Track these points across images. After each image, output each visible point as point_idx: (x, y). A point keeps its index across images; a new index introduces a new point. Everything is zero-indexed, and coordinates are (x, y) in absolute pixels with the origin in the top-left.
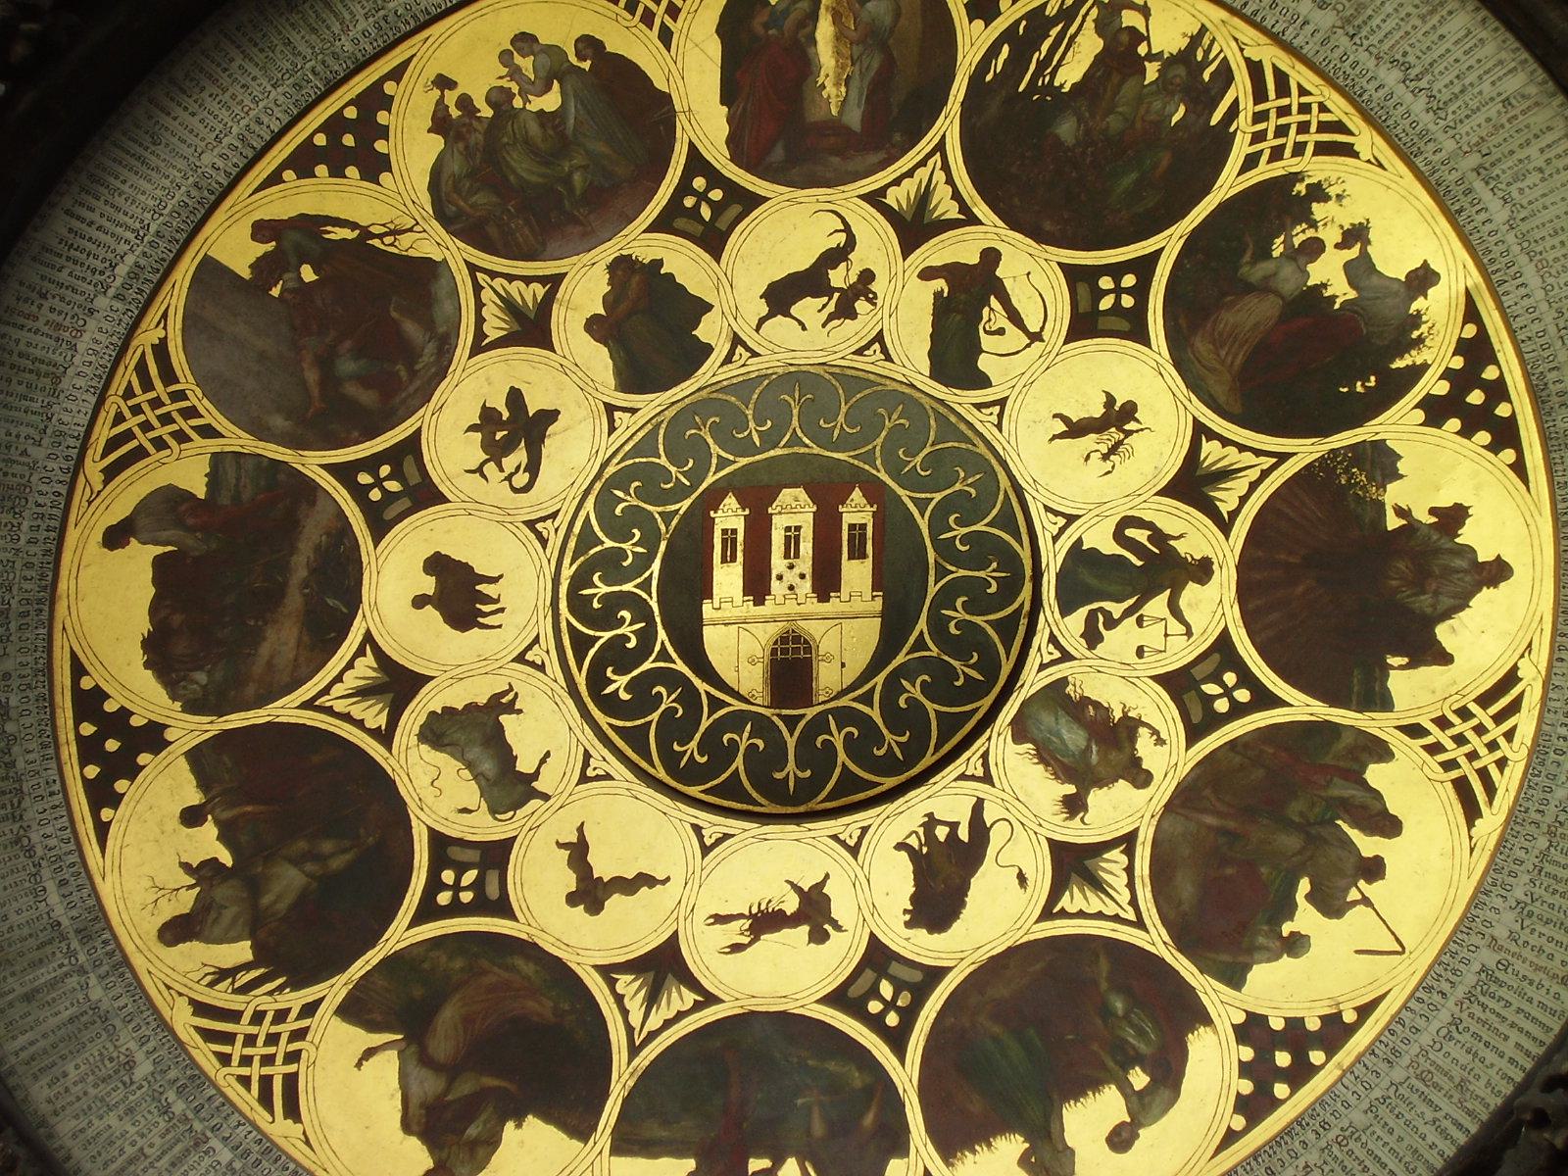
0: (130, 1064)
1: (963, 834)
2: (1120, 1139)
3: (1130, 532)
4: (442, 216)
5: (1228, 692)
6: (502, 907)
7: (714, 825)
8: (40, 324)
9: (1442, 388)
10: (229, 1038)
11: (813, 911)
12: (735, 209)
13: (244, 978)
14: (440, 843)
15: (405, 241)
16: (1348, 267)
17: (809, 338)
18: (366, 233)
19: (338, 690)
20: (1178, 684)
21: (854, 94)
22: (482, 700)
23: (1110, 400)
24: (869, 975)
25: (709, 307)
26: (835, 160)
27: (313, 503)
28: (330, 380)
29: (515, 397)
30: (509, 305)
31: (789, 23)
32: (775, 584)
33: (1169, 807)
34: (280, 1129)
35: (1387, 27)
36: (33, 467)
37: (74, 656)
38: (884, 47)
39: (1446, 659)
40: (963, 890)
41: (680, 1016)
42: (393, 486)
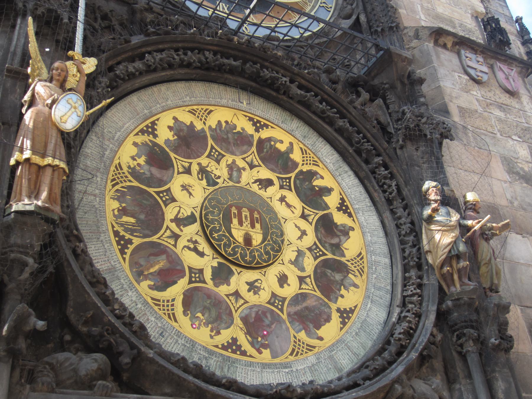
0: (375, 278)
1: (258, 183)
2: (282, 142)
4: (232, 322)
6: (315, 244)
7: (282, 221)
8: (305, 378)
9: (151, 136)
12: (193, 270)
14: (315, 258)
15: (241, 326)
16: (139, 158)
18: (245, 334)
19: (310, 288)
20: (218, 162)
21: (159, 259)
23: (182, 190)
26: (173, 257)
27: (290, 312)
29: (249, 291)
30: (236, 301)
33: (236, 155)
34: (364, 253)
35: (94, 162)
36: (325, 359)
37: (341, 331)
38: (148, 257)
39: (191, 122)
40: (264, 179)
41: (308, 210)
42: (277, 301)
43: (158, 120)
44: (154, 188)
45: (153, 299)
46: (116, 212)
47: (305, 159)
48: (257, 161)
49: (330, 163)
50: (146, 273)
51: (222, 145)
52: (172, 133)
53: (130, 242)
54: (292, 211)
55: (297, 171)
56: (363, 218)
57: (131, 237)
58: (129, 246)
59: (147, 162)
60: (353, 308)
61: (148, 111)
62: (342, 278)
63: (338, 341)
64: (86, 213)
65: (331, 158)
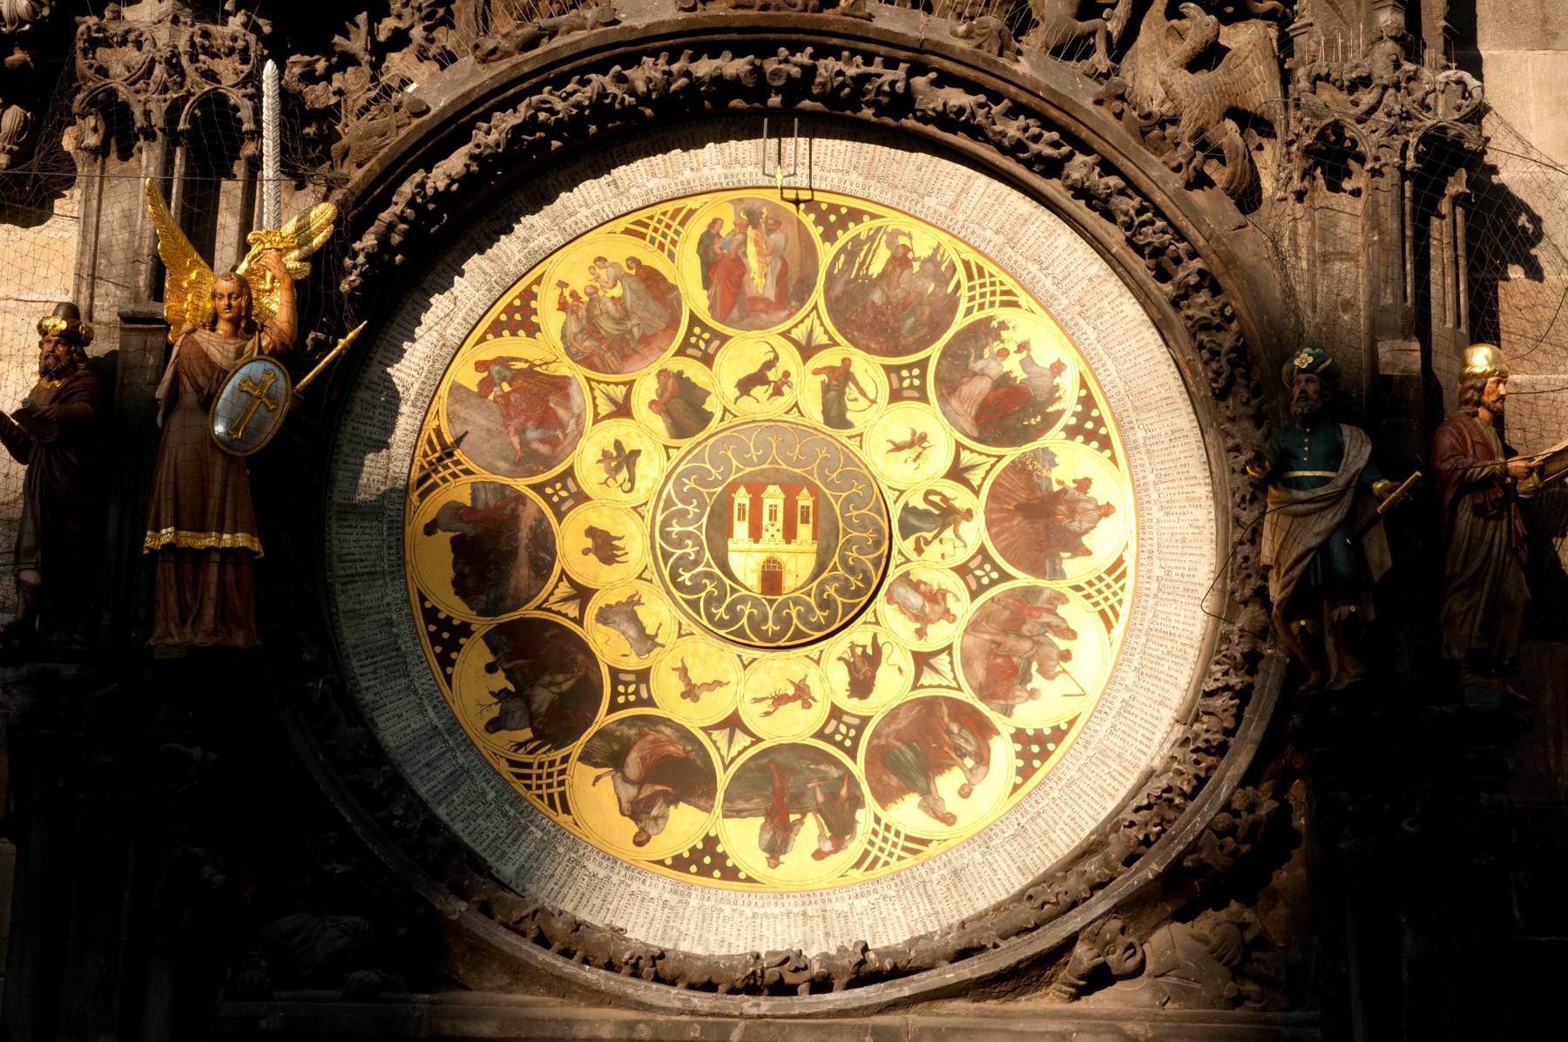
0: (484, 794)
1: (869, 651)
2: (965, 793)
3: (931, 497)
5: (987, 574)
6: (650, 702)
9: (1073, 421)
10: (529, 777)
11: (802, 693)
12: (716, 343)
13: (531, 746)
14: (614, 672)
16: (1022, 362)
17: (760, 404)
18: (533, 365)
19: (552, 599)
20: (962, 570)
22: (624, 600)
23: (914, 433)
24: (833, 723)
25: (708, 393)
26: (764, 316)
28: (525, 444)
31: (733, 246)
32: (764, 533)
33: (966, 631)
38: (783, 259)
39: (1088, 553)
40: (873, 677)
41: (745, 749)
42: (564, 494)
44: (939, 363)
45: (691, 212)
46: (902, 240)
47: (891, 836)
48: (931, 686)
51: (1005, 608)
53: (829, 236)
54: (762, 699)
55: (865, 788)
56: (654, 894)
58: (821, 229)
59: (1006, 377)
60: (449, 670)
61: (1141, 441)
62: (534, 707)
63: (401, 561)
65: (867, 923)
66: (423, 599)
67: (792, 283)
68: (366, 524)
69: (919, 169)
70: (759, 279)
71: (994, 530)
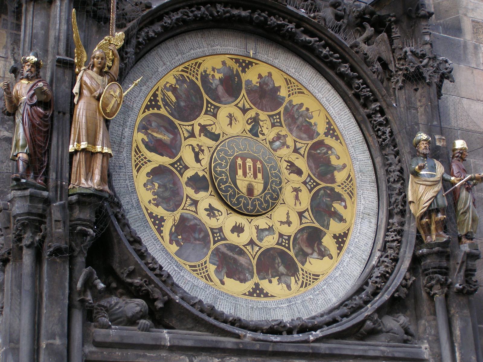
0: (310, 298)
1: (289, 164)
4: (173, 211)
6: (289, 237)
9: (241, 68)
10: (306, 283)
14: (278, 244)
15: (176, 219)
17: (205, 158)
20: (273, 125)
22: (256, 231)
23: (227, 116)
24: (307, 185)
28: (199, 240)
29: (206, 210)
30: (191, 205)
31: (152, 140)
36: (210, 293)
39: (280, 87)
41: (309, 214)
43: (256, 64)
44: (209, 97)
45: (137, 146)
46: (168, 85)
48: (304, 152)
49: (363, 204)
50: (149, 131)
52: (259, 80)
53: (159, 108)
56: (348, 259)
57: (162, 106)
58: (155, 109)
62: (285, 273)
64: (149, 67)
66: (245, 294)
67: (169, 127)
68: (218, 303)
69: (149, 67)
70: (166, 137)
71: (264, 109)
